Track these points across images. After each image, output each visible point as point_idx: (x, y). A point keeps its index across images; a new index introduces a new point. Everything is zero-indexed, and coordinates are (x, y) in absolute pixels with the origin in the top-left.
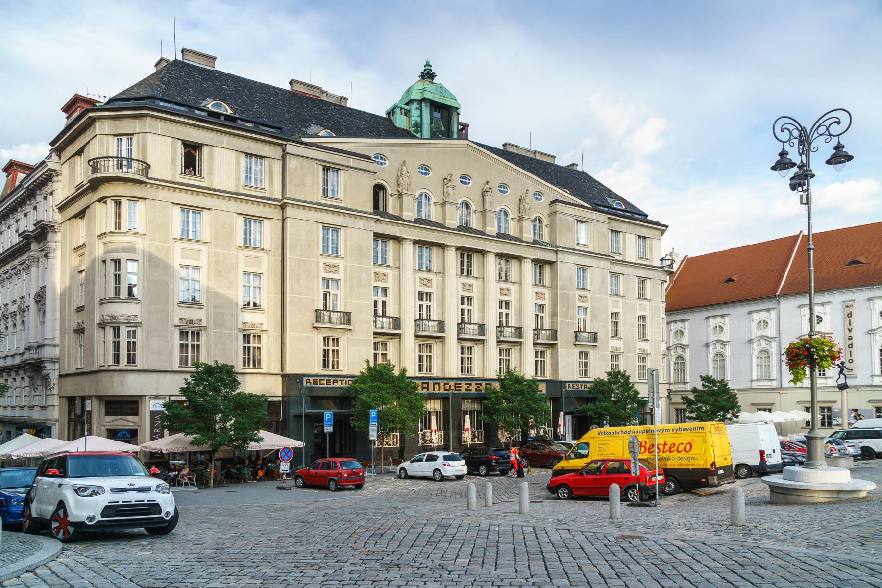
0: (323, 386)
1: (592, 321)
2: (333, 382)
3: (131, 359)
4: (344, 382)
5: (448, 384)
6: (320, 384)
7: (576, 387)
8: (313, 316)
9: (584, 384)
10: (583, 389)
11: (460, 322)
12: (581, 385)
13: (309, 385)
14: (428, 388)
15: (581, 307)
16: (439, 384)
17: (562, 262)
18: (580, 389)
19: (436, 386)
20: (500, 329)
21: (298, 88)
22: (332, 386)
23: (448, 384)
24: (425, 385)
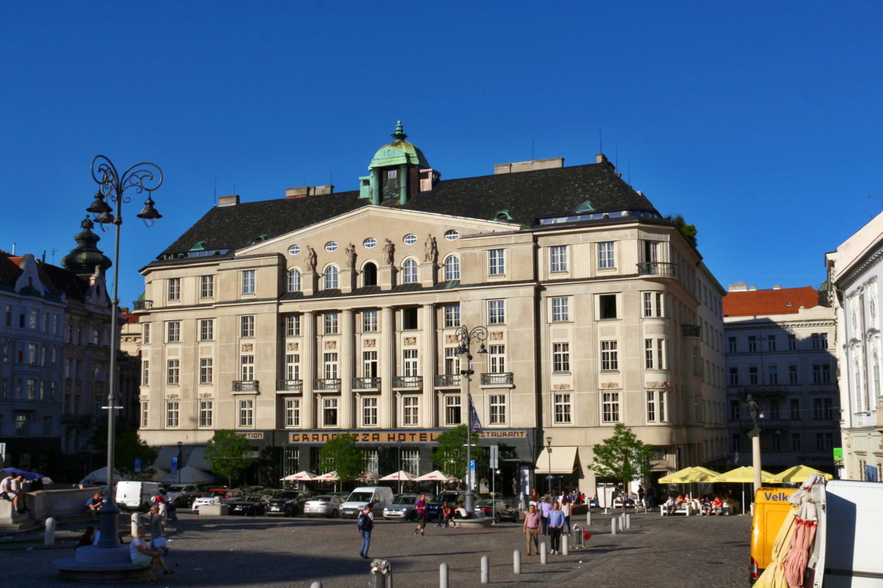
1: (509, 359)
3: (146, 424)
8: (231, 386)
9: (491, 432)
10: (490, 437)
12: (488, 433)
14: (317, 439)
16: (327, 435)
17: (465, 301)
18: (486, 437)
19: (325, 437)
24: (315, 437)
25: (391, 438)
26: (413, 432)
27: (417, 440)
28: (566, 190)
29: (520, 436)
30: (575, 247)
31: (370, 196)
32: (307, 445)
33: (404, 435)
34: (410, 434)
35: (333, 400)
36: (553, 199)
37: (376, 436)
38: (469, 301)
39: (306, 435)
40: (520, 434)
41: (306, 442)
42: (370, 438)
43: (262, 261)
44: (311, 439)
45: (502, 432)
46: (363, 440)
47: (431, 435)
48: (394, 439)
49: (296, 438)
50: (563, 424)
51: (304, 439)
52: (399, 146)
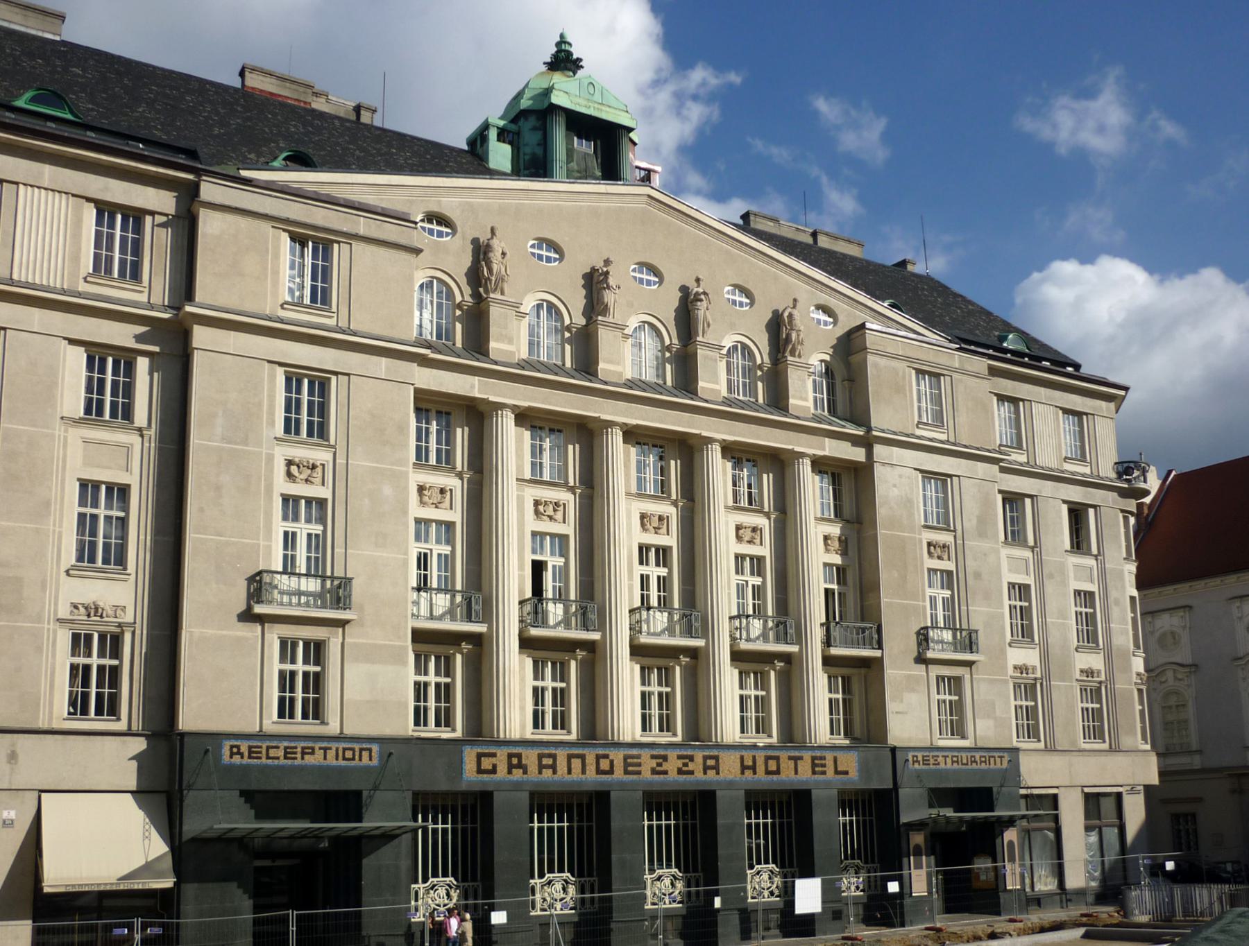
0: (276, 762)
2: (303, 753)
4: (331, 754)
5: (606, 756)
6: (268, 757)
7: (932, 761)
9: (950, 754)
10: (949, 766)
11: (638, 603)
12: (945, 757)
13: (237, 759)
14: (554, 768)
15: (935, 571)
16: (582, 757)
18: (942, 766)
19: (576, 763)
20: (737, 623)
21: (253, 81)
22: (296, 762)
23: (606, 756)
24: (546, 761)
25: (748, 768)
29: (999, 765)
32: (517, 786)
33: (777, 758)
34: (790, 758)
39: (519, 756)
40: (998, 760)
42: (696, 766)
44: (533, 767)
45: (969, 755)
46: (680, 772)
48: (754, 768)
49: (487, 763)
51: (511, 768)
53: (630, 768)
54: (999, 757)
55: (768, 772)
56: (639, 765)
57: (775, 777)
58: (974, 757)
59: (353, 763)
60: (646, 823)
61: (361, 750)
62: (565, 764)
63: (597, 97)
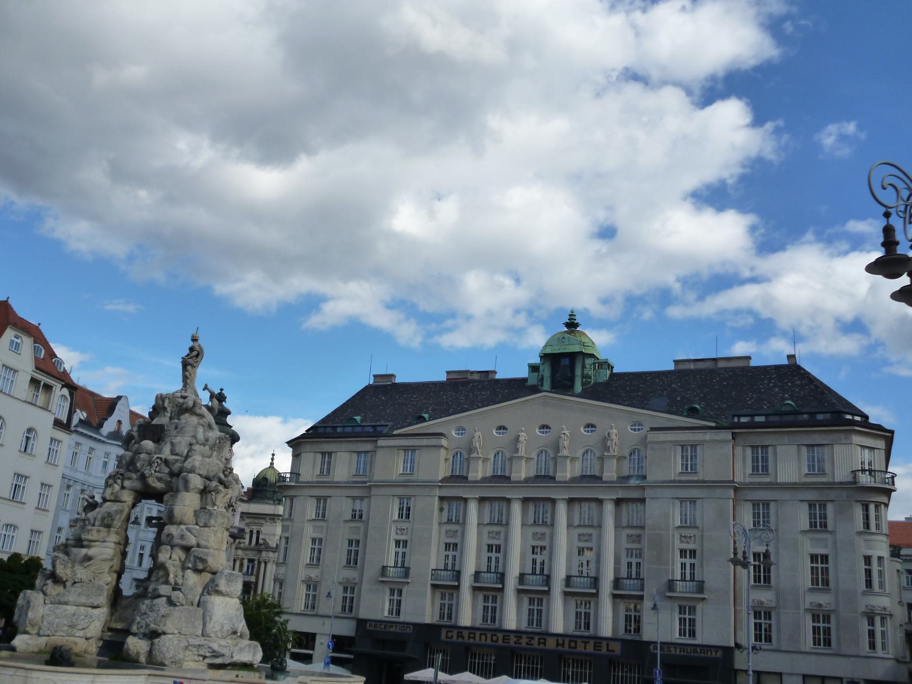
2: (390, 628)
4: (398, 628)
5: (495, 635)
7: (666, 649)
9: (679, 647)
12: (675, 649)
14: (474, 638)
16: (486, 635)
17: (651, 498)
18: (673, 652)
19: (483, 637)
22: (388, 630)
24: (472, 635)
26: (586, 640)
27: (590, 648)
28: (761, 389)
30: (779, 448)
31: (540, 383)
35: (538, 599)
36: (748, 397)
37: (542, 641)
38: (657, 498)
39: (461, 633)
40: (714, 653)
41: (460, 640)
42: (535, 642)
43: (425, 442)
44: (466, 637)
47: (608, 645)
48: (563, 645)
49: (450, 635)
50: (764, 645)
52: (573, 334)
53: (506, 641)
54: (714, 651)
55: (570, 647)
56: (509, 639)
57: (574, 650)
58: (696, 650)
59: (404, 632)
60: (449, 658)
61: (407, 627)
62: (479, 637)
63: (566, 343)
